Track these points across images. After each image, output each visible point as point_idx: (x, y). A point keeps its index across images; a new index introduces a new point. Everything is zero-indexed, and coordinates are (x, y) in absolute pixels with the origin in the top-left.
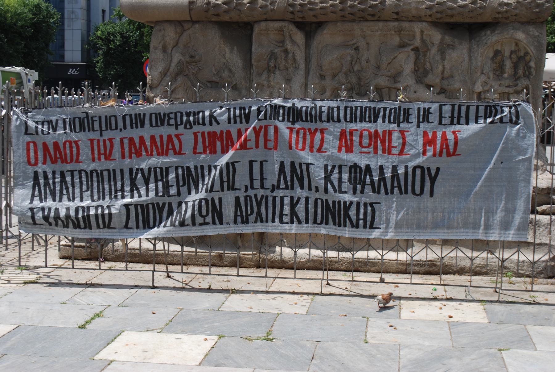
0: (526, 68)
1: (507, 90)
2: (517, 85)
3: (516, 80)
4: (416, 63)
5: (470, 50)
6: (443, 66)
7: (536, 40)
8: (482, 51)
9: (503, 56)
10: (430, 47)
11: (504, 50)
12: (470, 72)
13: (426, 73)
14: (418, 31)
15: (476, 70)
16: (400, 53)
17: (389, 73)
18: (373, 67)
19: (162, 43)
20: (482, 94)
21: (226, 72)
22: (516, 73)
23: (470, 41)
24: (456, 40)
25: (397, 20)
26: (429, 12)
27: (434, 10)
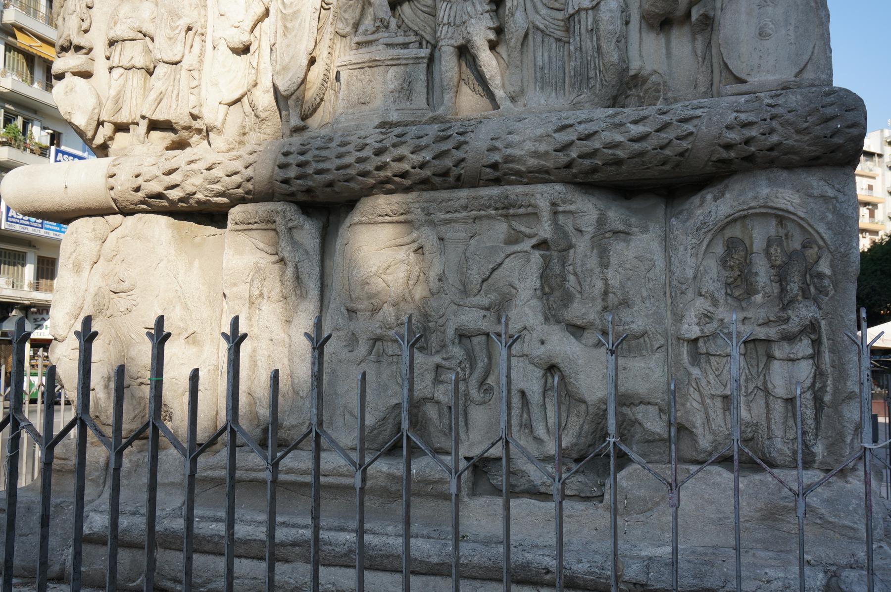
0: (808, 277)
1: (762, 333)
2: (787, 320)
3: (784, 308)
4: (544, 276)
5: (666, 243)
6: (605, 280)
7: (831, 207)
8: (694, 241)
9: (748, 252)
10: (574, 240)
11: (751, 237)
12: (671, 294)
13: (567, 299)
14: (544, 205)
15: (684, 287)
16: (508, 256)
17: (485, 302)
18: (453, 289)
19: (73, 257)
20: (701, 343)
21: (178, 307)
22: (783, 290)
23: (667, 218)
24: (633, 220)
25: (497, 181)
26: (562, 158)
27: (574, 155)
